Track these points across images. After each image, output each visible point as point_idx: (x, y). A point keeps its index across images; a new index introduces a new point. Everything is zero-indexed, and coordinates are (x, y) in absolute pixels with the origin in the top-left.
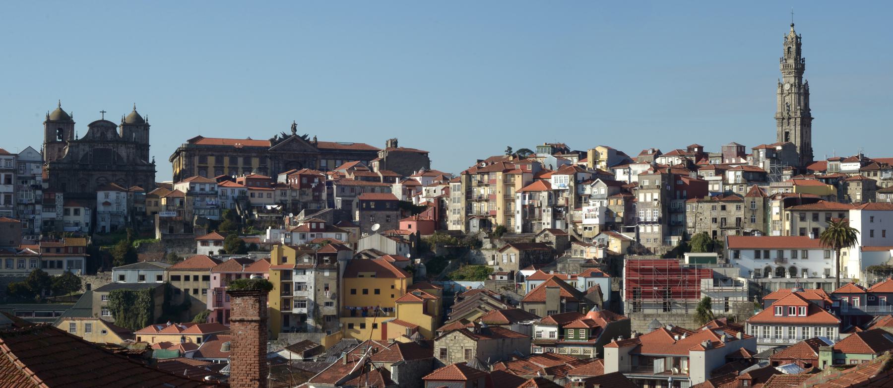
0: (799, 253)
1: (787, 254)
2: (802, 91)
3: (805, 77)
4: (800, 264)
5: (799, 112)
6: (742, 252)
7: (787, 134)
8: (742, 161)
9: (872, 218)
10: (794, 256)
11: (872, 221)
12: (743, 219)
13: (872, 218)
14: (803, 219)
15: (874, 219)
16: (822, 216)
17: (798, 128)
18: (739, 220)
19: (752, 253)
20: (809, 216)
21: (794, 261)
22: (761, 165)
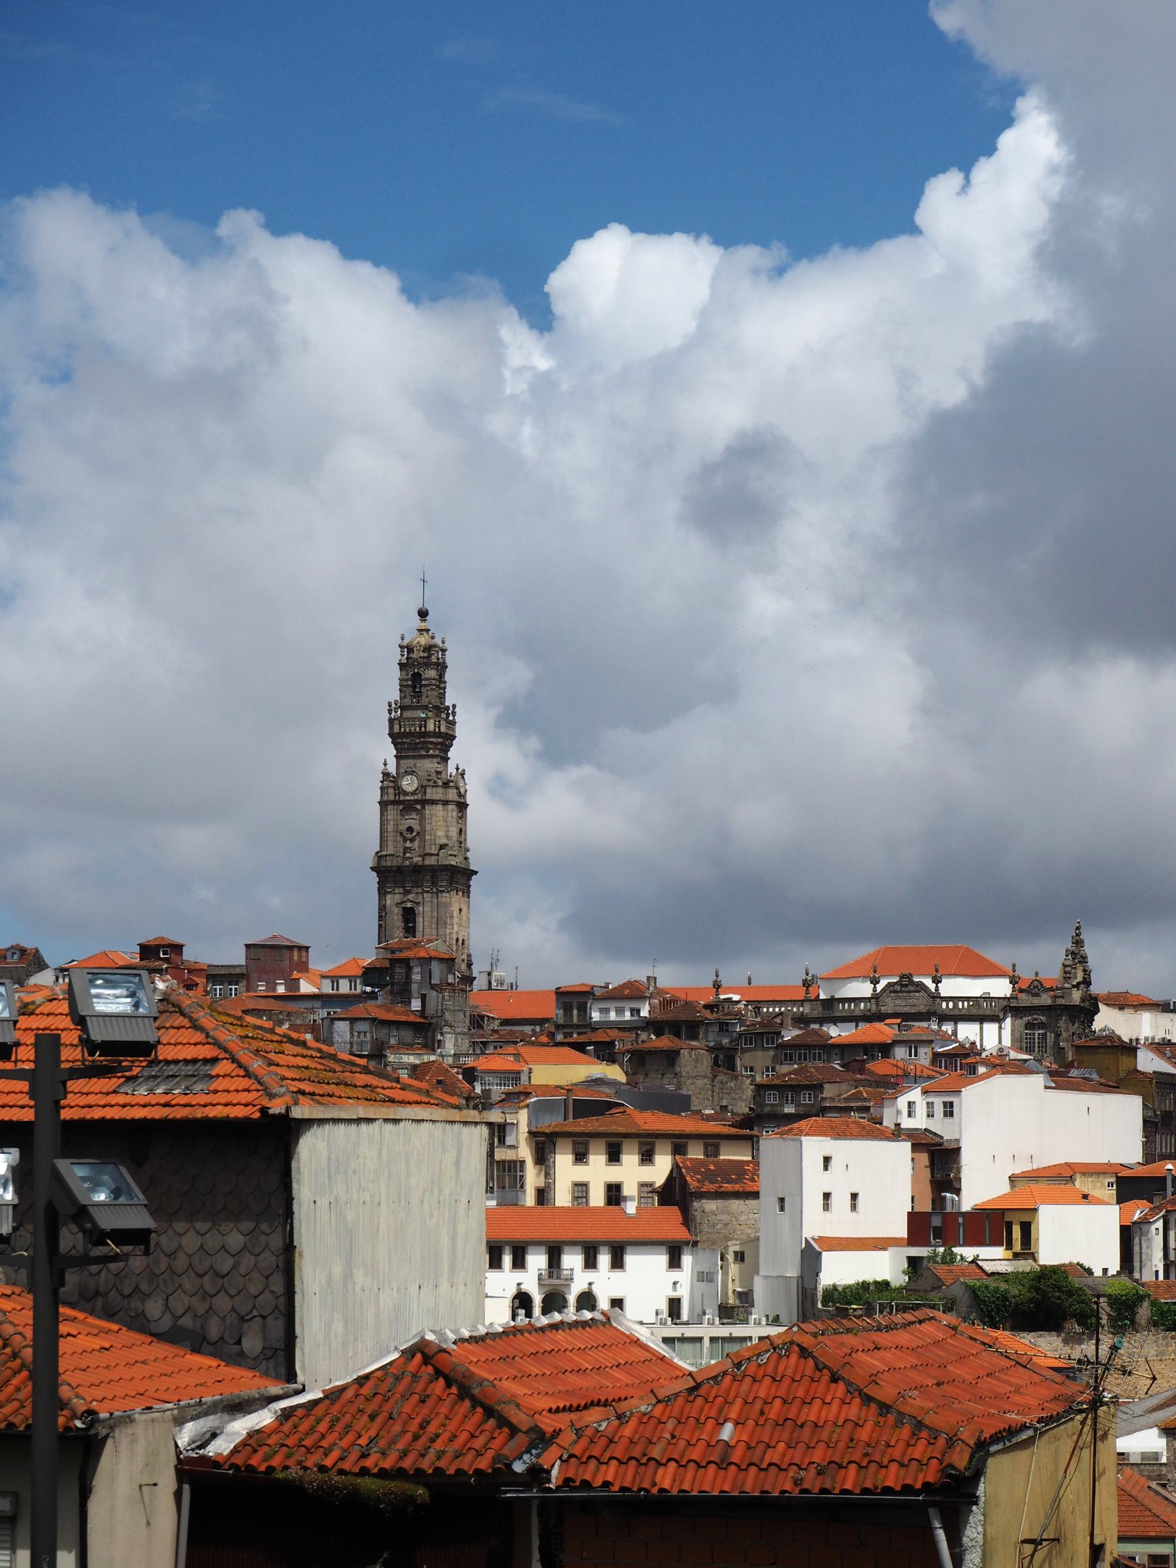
4: (605, 1282)
7: (409, 916)
9: (827, 1160)
10: (590, 1263)
11: (826, 1168)
13: (827, 1160)
14: (580, 1157)
15: (833, 1163)
21: (590, 1276)
22: (416, 1005)
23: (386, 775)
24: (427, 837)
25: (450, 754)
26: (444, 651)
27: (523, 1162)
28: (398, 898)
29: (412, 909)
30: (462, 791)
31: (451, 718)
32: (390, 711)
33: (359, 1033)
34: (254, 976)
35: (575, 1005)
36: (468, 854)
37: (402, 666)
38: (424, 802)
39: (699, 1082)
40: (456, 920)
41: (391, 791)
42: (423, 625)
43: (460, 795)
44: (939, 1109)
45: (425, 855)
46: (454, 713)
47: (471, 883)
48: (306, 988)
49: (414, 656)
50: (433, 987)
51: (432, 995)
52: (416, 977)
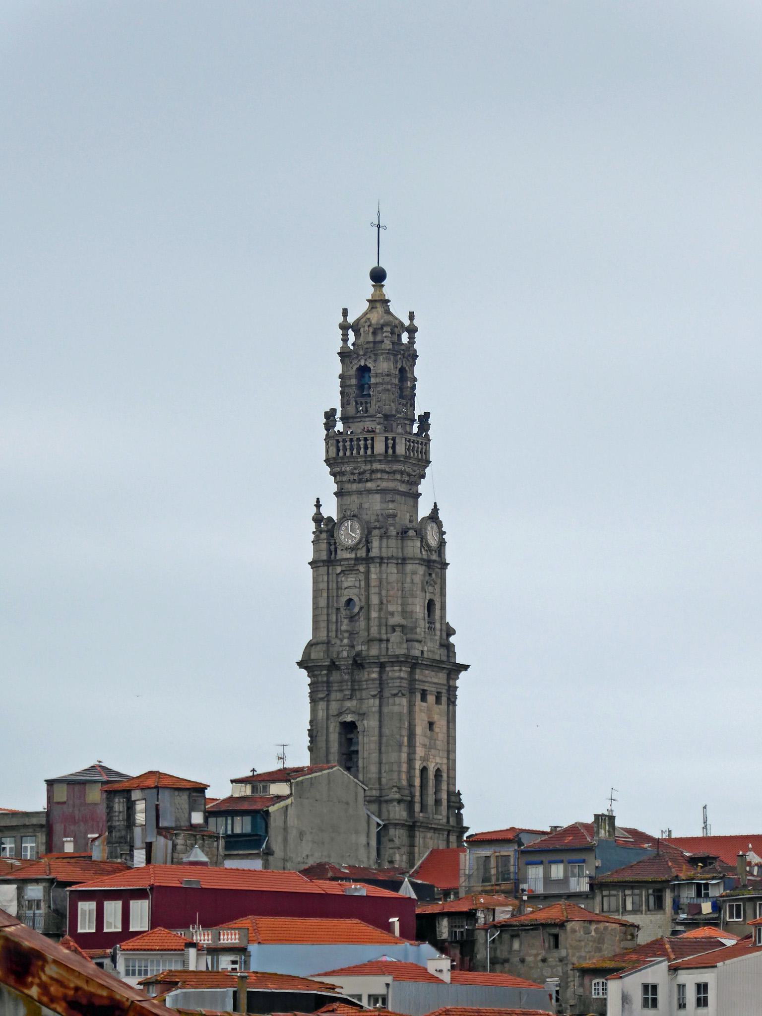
22: (140, 857)
24: (374, 614)
25: (421, 489)
26: (412, 330)
28: (334, 707)
30: (433, 541)
34: (58, 828)
36: (452, 639)
37: (344, 355)
38: (368, 560)
40: (419, 740)
41: (324, 546)
43: (429, 549)
44: (691, 995)
45: (370, 641)
47: (458, 683)
49: (362, 339)
50: (161, 831)
51: (161, 844)
52: (140, 818)
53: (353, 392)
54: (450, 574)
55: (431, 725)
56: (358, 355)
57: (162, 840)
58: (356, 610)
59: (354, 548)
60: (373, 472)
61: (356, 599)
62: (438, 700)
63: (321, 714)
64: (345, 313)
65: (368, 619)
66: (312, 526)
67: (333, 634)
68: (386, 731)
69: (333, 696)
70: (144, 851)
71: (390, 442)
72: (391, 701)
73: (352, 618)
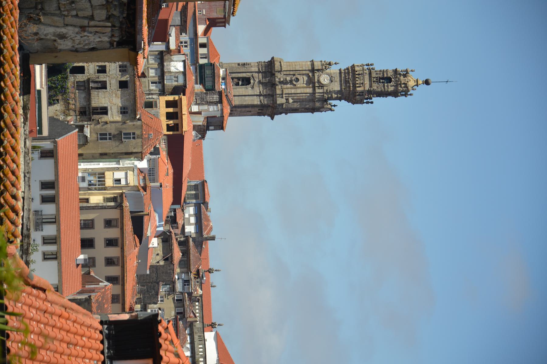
0: (52, 248)
1: (50, 230)
2: (318, 104)
3: (342, 106)
5: (283, 101)
6: (50, 162)
7: (246, 81)
8: (201, 28)
12: (105, 118)
14: (108, 223)
16: (113, 252)
17: (256, 101)
18: (104, 111)
19: (49, 177)
20: (113, 233)
22: (195, 108)
23: (330, 64)
25: (343, 101)
26: (406, 95)
27: (105, 189)
29: (249, 83)
30: (321, 110)
31: (365, 101)
32: (368, 65)
33: (177, 77)
35: (197, 192)
37: (396, 71)
38: (314, 88)
39: (154, 275)
40: (243, 109)
41: (320, 68)
42: (420, 82)
46: (367, 103)
47: (266, 116)
48: (201, 28)
49: (402, 77)
52: (212, 108)
53: (381, 76)
54: (310, 114)
55: (250, 111)
56: (396, 78)
57: (202, 119)
58: (294, 83)
59: (319, 82)
60: (350, 87)
61: (299, 83)
62: (258, 113)
63: (253, 69)
64: (412, 71)
65: (291, 88)
66: (328, 61)
67: (285, 73)
68: (247, 98)
69: (260, 74)
70: (198, 111)
71: (361, 94)
72: (259, 100)
73: (291, 81)
